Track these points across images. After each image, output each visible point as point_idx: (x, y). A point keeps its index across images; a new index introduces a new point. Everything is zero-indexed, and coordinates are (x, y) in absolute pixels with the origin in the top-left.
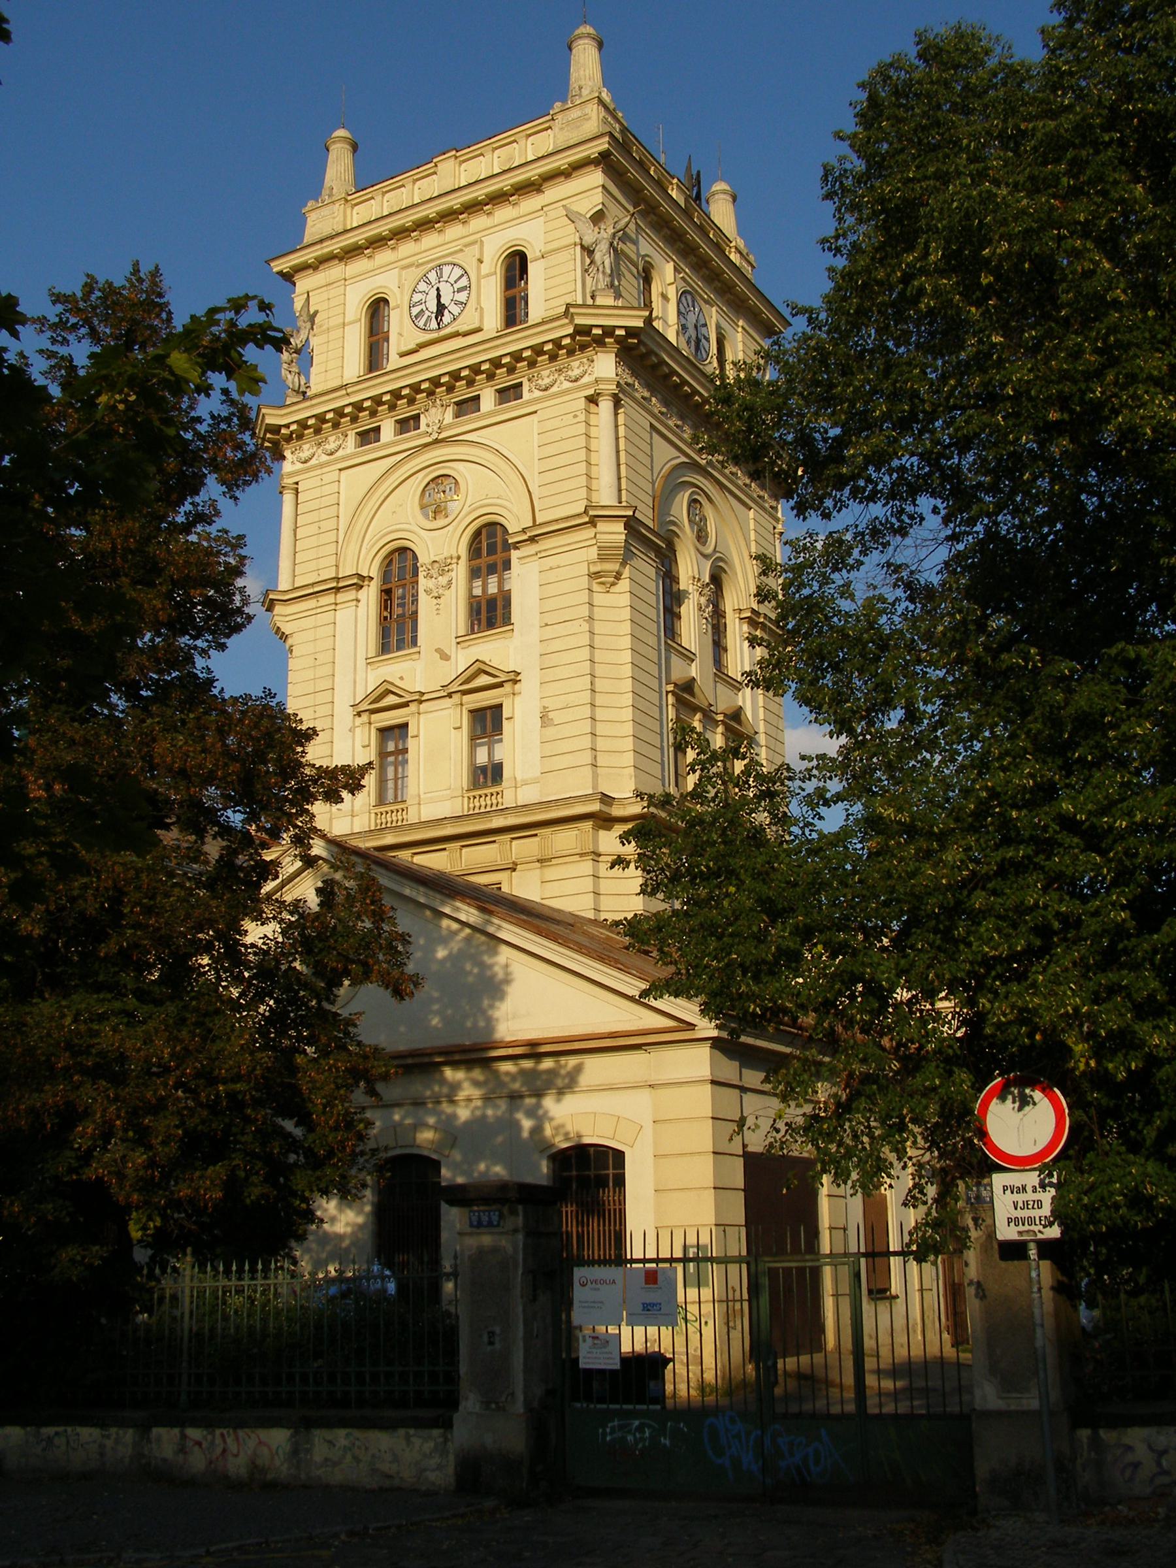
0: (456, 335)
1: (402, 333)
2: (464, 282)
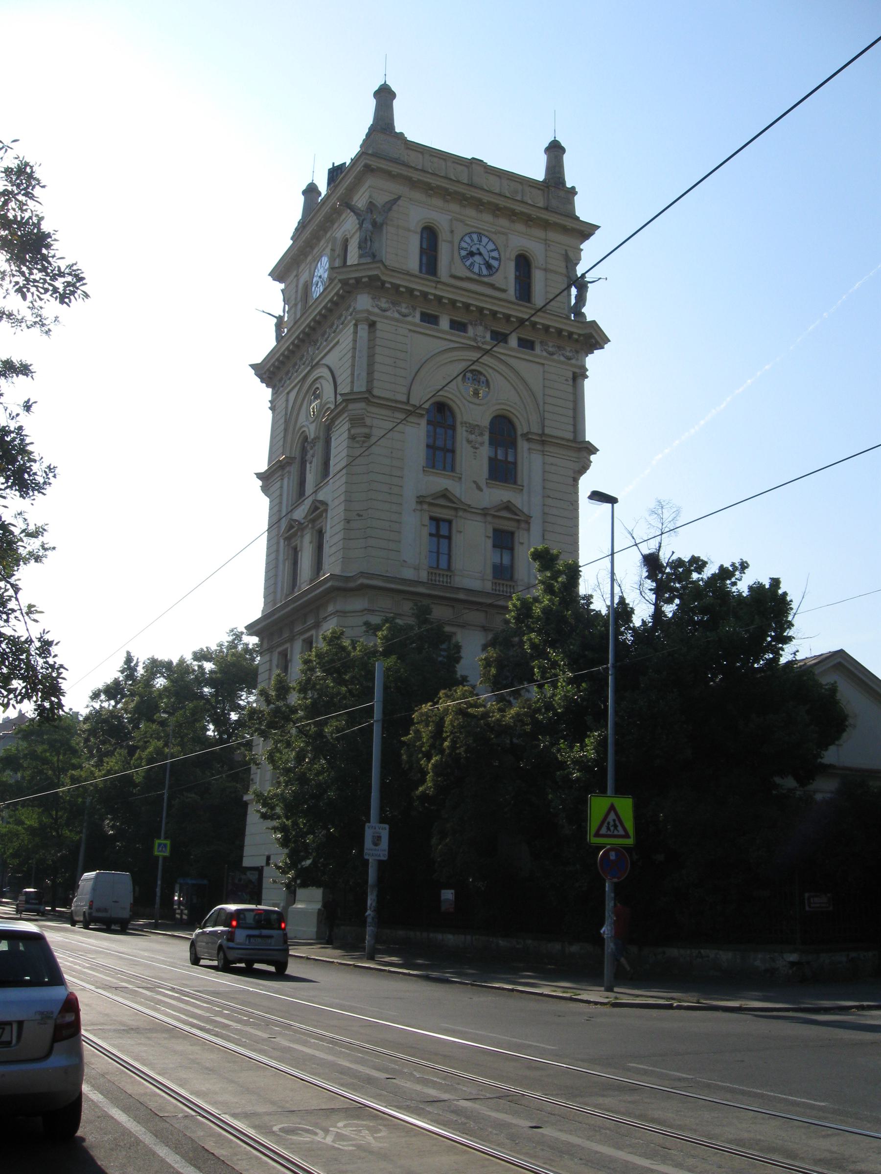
0: (492, 286)
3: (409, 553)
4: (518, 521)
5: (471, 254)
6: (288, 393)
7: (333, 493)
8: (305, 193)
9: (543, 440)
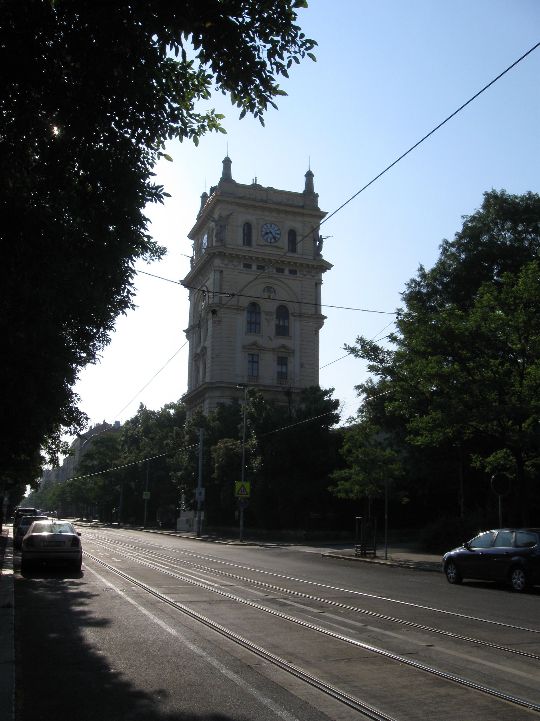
0: (277, 247)
2: (278, 232)
3: (240, 369)
4: (289, 353)
5: (267, 233)
6: (195, 295)
7: (208, 344)
8: (223, 162)
9: (300, 315)
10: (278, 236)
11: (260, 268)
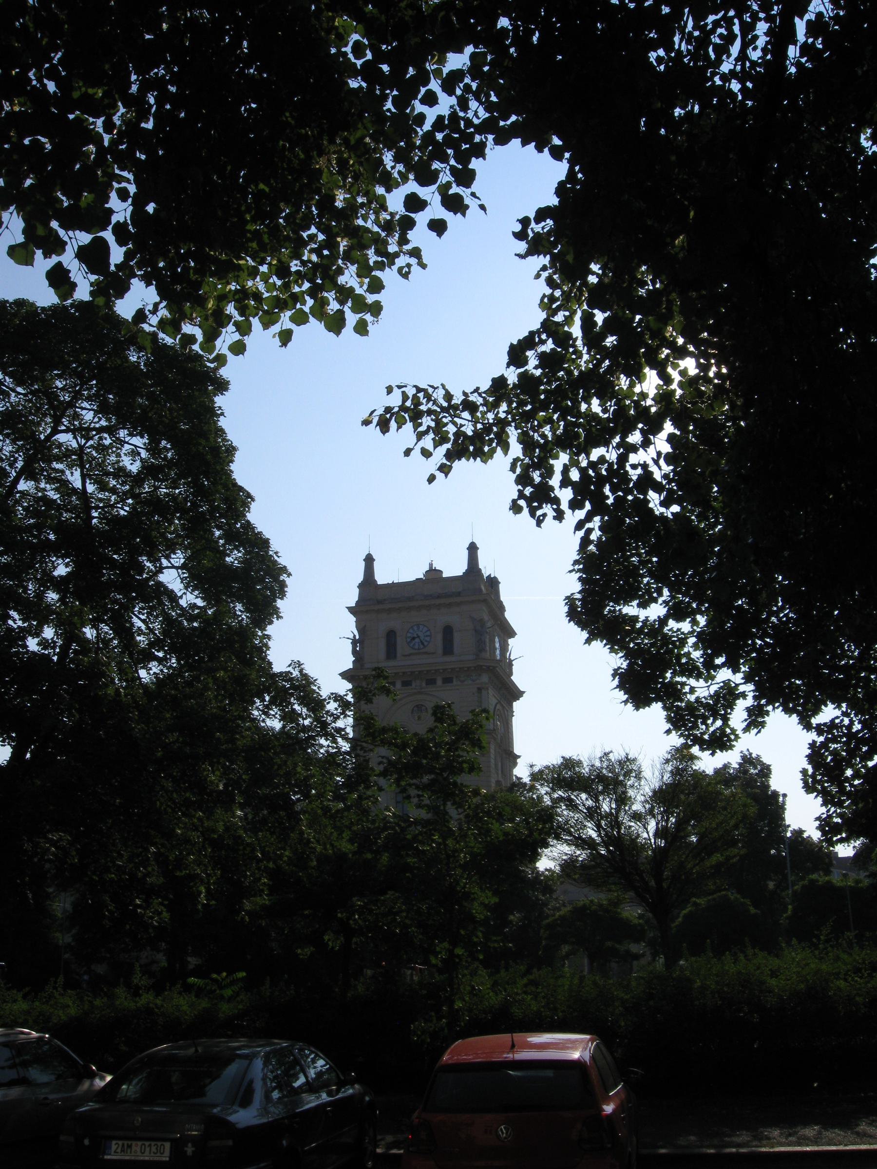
0: (426, 653)
1: (402, 646)
2: (428, 633)
5: (414, 638)
10: (428, 639)
11: (406, 684)
